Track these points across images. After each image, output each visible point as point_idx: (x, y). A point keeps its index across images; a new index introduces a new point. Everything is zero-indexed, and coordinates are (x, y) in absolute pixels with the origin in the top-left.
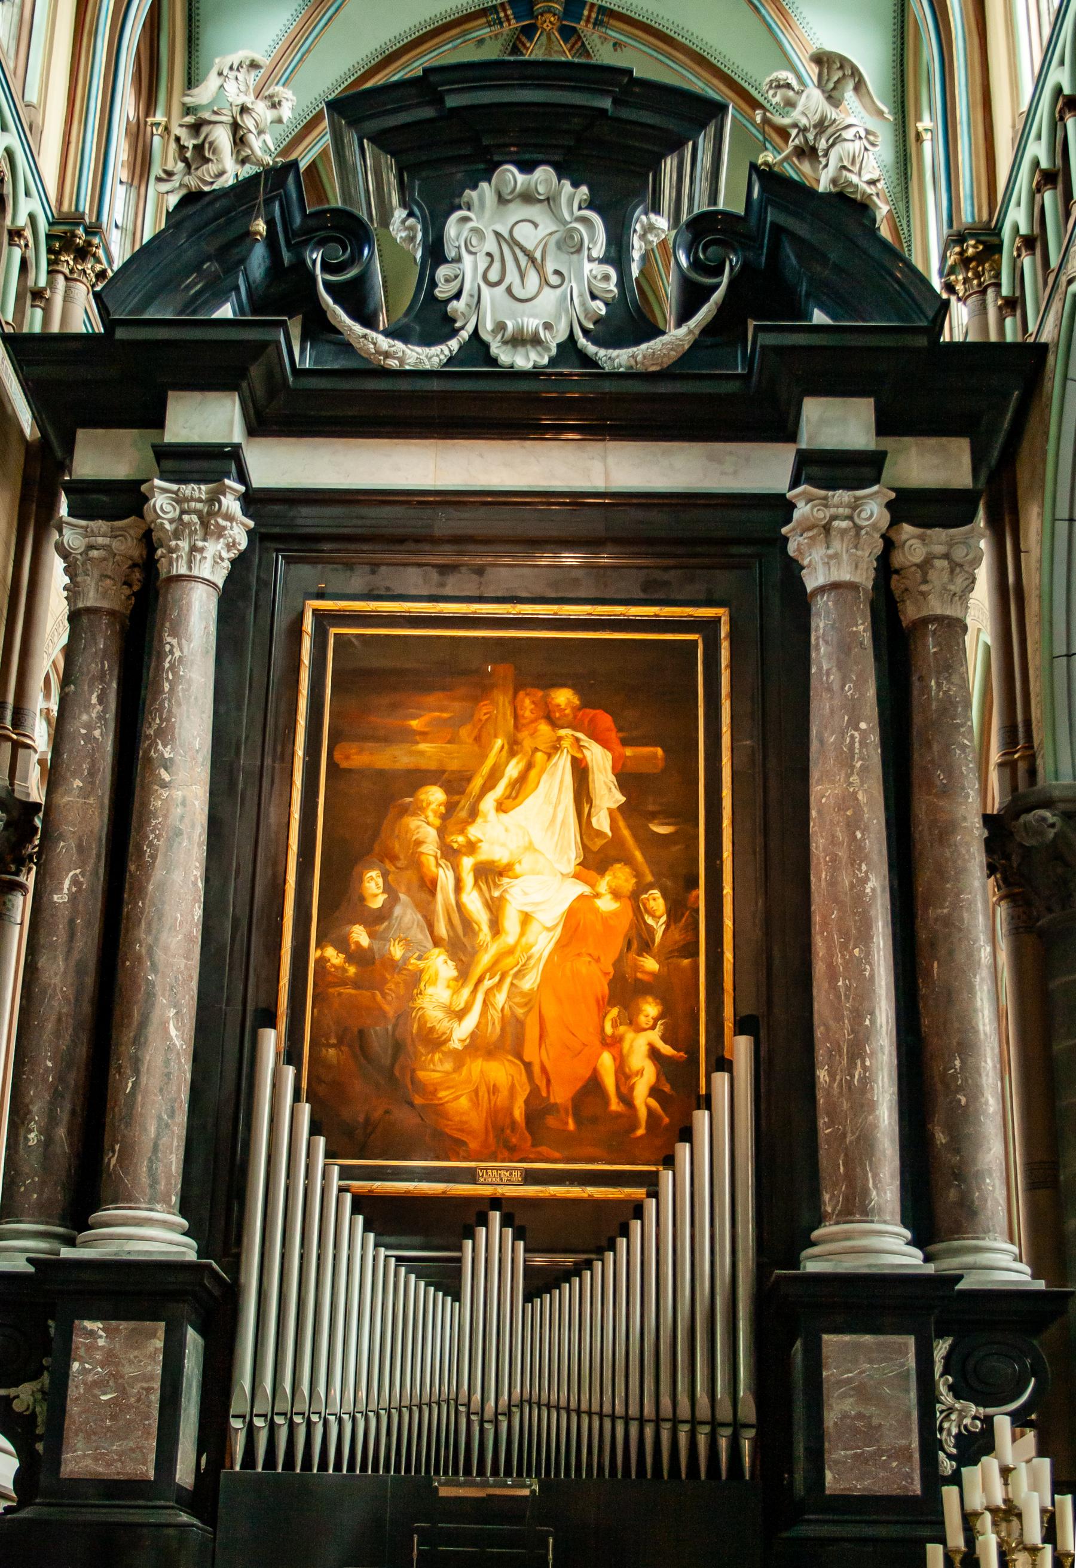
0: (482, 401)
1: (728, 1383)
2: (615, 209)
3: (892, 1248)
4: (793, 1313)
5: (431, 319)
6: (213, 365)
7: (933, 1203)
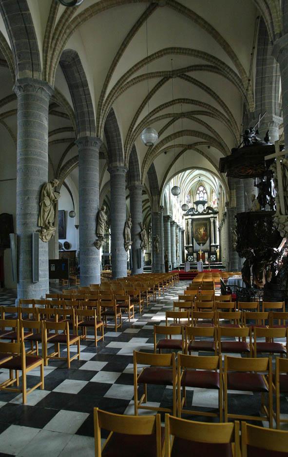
0: (199, 214)
1: (209, 248)
2: (204, 206)
3: (213, 244)
4: (211, 246)
5: (197, 211)
6: (190, 215)
7: (215, 243)
